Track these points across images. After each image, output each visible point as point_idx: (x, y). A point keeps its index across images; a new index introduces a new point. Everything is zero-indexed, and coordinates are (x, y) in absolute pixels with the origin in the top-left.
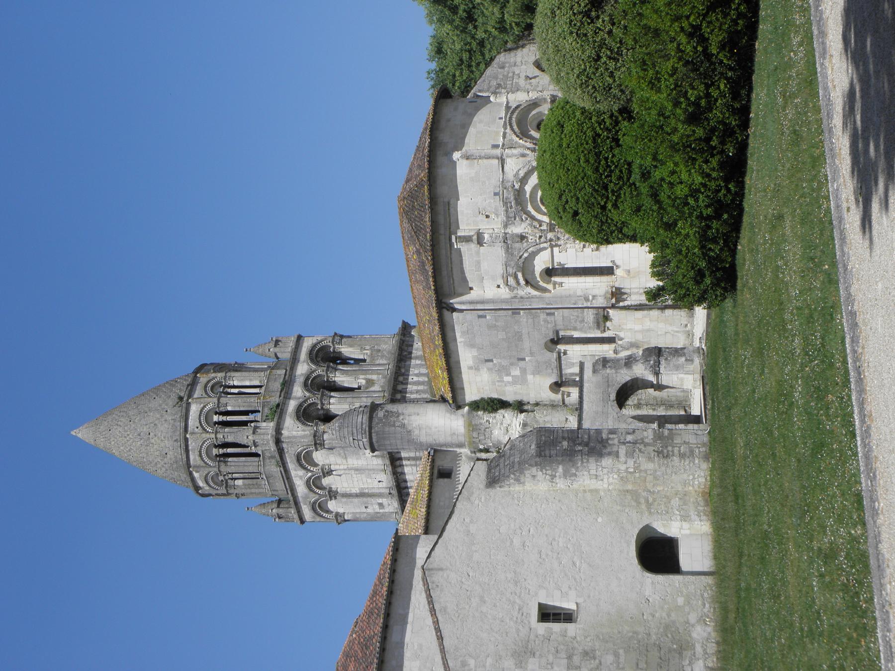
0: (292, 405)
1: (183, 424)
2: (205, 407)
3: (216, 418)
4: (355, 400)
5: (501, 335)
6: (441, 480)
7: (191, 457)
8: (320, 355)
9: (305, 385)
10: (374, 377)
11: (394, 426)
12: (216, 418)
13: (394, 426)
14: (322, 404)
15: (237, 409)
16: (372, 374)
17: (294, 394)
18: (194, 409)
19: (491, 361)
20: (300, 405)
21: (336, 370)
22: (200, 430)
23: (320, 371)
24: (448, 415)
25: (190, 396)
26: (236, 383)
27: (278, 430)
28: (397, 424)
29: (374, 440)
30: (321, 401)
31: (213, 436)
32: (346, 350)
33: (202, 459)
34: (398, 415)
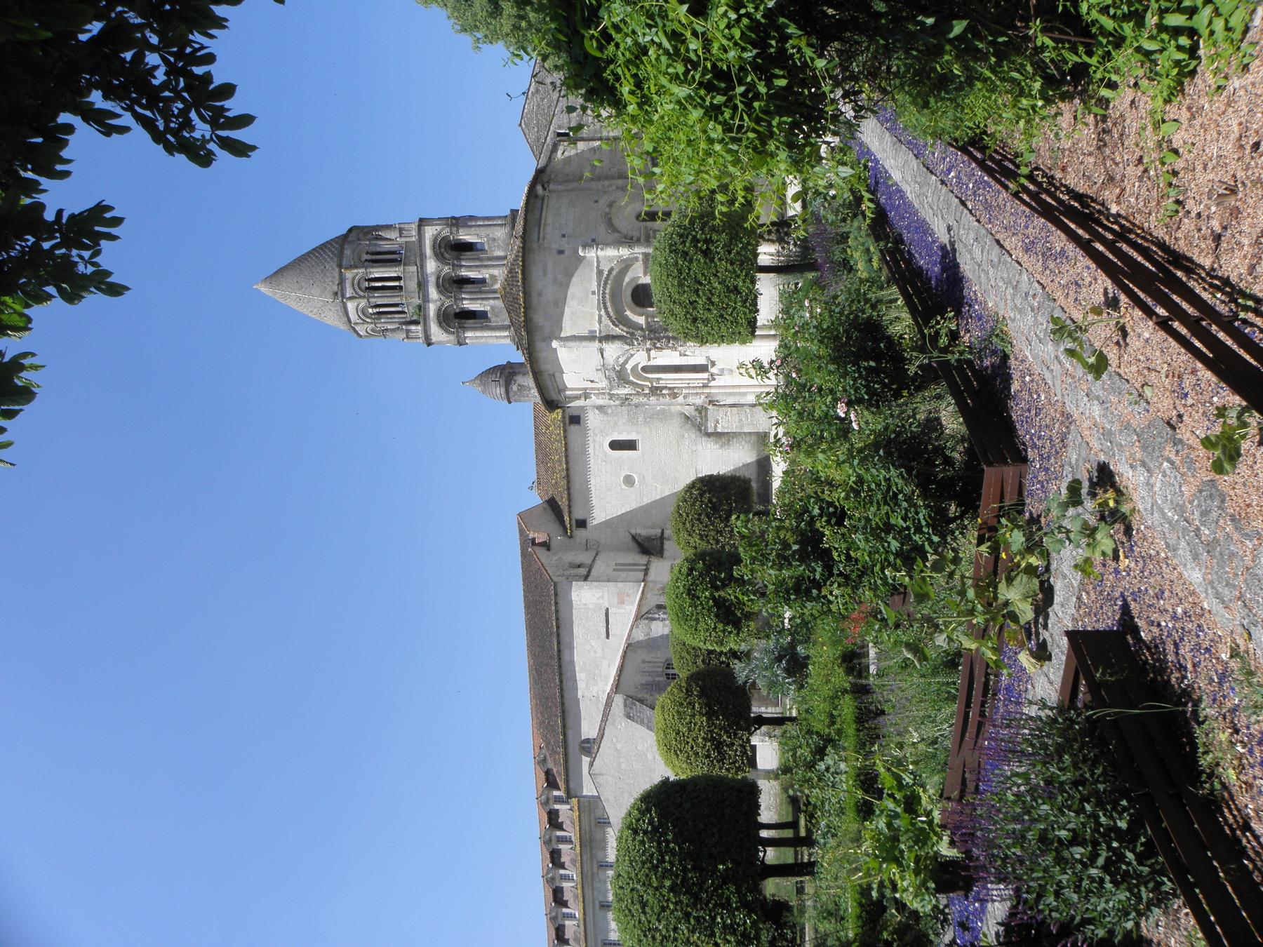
0: (432, 309)
18: (351, 306)
20: (439, 310)
21: (462, 266)
23: (447, 269)
25: (343, 296)
32: (466, 236)
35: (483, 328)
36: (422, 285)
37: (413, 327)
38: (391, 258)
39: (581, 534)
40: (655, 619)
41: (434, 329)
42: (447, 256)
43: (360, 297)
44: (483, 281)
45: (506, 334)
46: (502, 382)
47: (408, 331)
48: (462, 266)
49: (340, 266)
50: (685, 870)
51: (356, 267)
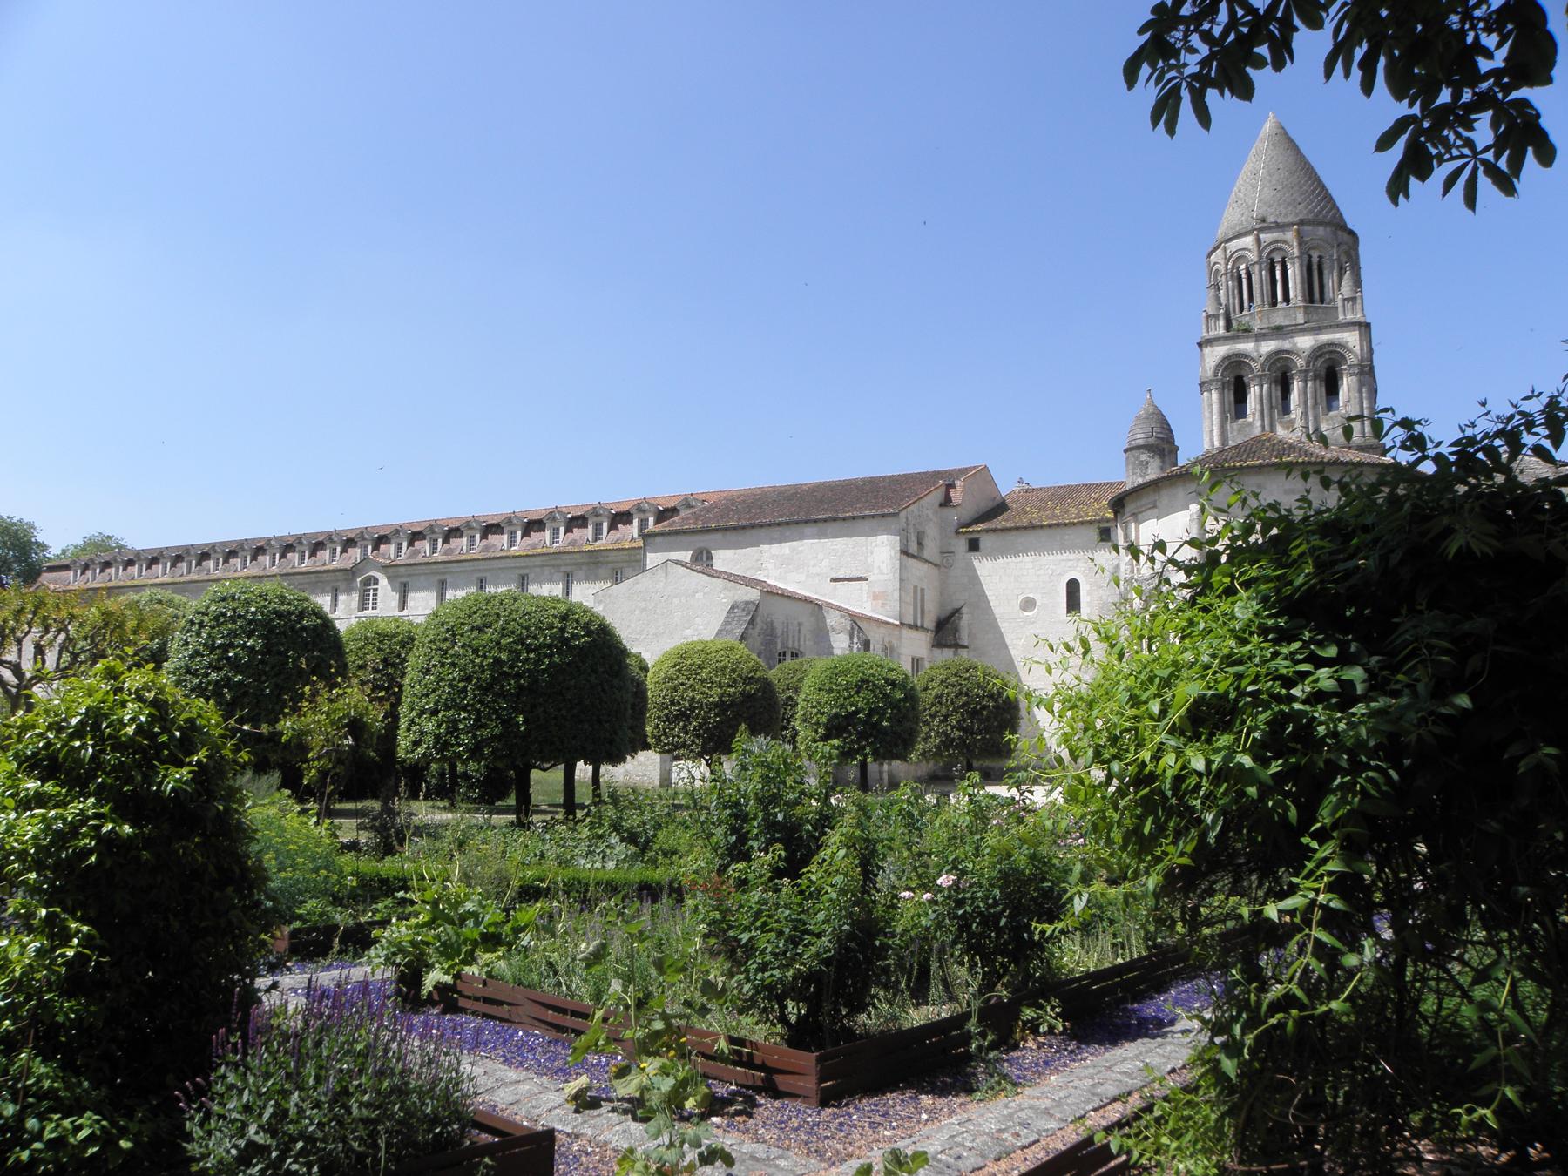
0: (1247, 346)
3: (1243, 267)
9: (1278, 352)
18: (1248, 241)
20: (1246, 356)
21: (1305, 382)
23: (1300, 363)
25: (1261, 230)
32: (1347, 386)
35: (1223, 413)
36: (1278, 331)
37: (1222, 323)
38: (1314, 293)
39: (961, 545)
40: (851, 638)
41: (1221, 351)
42: (1320, 361)
43: (1260, 253)
44: (1286, 410)
45: (1217, 444)
46: (1152, 441)
47: (1216, 317)
48: (1305, 382)
49: (1301, 223)
50: (518, 676)
51: (1300, 244)
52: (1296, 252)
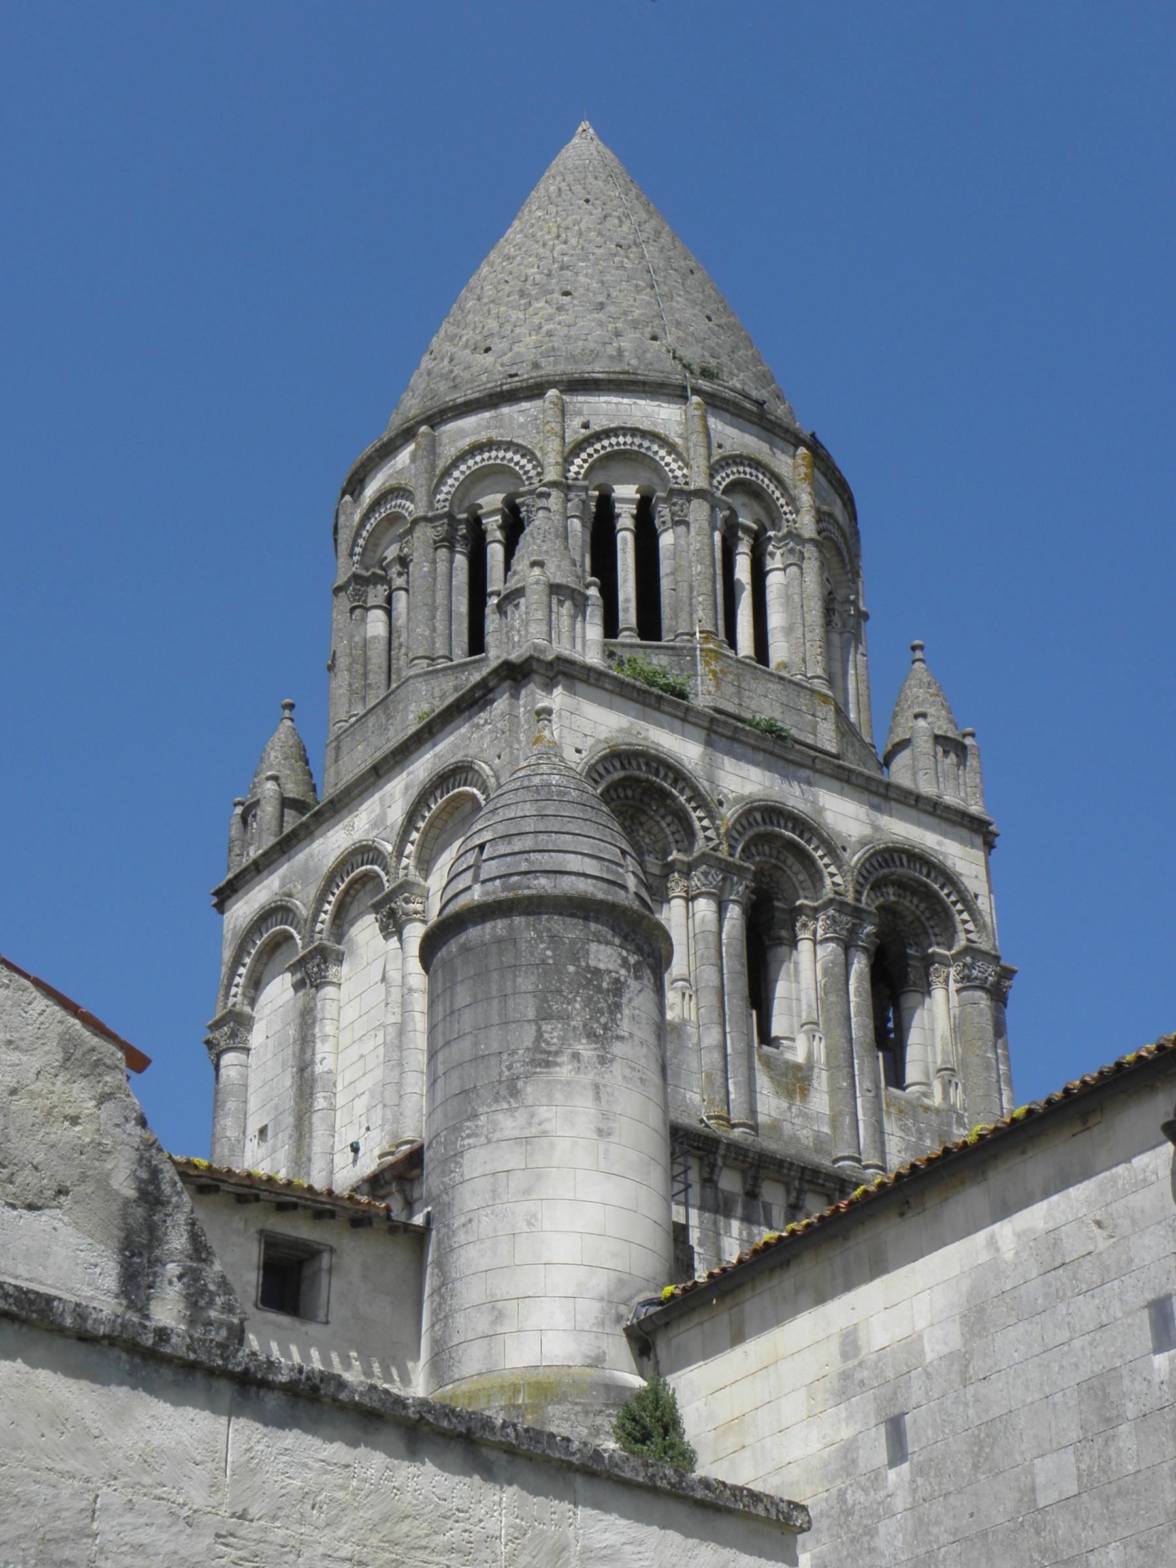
1: (598, 369)
2: (672, 448)
3: (626, 492)
4: (709, 999)
5: (1055, 1476)
6: (253, 1253)
7: (469, 422)
8: (910, 904)
9: (773, 812)
10: (820, 1101)
11: (545, 1015)
12: (626, 492)
13: (545, 1015)
14: (687, 871)
15: (665, 567)
16: (833, 1091)
17: (728, 762)
18: (664, 415)
19: (898, 1451)
21: (847, 946)
22: (574, 430)
23: (836, 880)
24: (601, 1282)
25: (715, 403)
26: (775, 581)
27: (564, 672)
28: (554, 1032)
29: (474, 934)
30: (704, 858)
31: (552, 475)
33: (462, 458)
34: (602, 1036)
36: (772, 745)
52: (806, 524)
